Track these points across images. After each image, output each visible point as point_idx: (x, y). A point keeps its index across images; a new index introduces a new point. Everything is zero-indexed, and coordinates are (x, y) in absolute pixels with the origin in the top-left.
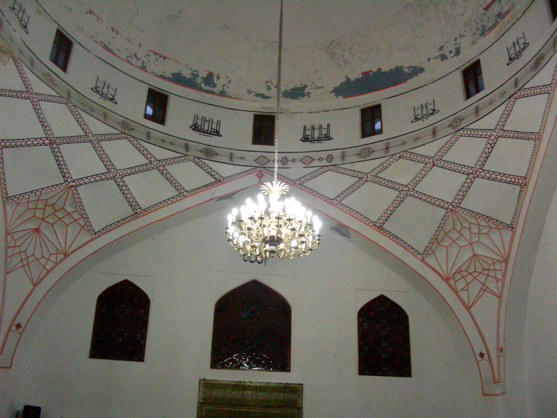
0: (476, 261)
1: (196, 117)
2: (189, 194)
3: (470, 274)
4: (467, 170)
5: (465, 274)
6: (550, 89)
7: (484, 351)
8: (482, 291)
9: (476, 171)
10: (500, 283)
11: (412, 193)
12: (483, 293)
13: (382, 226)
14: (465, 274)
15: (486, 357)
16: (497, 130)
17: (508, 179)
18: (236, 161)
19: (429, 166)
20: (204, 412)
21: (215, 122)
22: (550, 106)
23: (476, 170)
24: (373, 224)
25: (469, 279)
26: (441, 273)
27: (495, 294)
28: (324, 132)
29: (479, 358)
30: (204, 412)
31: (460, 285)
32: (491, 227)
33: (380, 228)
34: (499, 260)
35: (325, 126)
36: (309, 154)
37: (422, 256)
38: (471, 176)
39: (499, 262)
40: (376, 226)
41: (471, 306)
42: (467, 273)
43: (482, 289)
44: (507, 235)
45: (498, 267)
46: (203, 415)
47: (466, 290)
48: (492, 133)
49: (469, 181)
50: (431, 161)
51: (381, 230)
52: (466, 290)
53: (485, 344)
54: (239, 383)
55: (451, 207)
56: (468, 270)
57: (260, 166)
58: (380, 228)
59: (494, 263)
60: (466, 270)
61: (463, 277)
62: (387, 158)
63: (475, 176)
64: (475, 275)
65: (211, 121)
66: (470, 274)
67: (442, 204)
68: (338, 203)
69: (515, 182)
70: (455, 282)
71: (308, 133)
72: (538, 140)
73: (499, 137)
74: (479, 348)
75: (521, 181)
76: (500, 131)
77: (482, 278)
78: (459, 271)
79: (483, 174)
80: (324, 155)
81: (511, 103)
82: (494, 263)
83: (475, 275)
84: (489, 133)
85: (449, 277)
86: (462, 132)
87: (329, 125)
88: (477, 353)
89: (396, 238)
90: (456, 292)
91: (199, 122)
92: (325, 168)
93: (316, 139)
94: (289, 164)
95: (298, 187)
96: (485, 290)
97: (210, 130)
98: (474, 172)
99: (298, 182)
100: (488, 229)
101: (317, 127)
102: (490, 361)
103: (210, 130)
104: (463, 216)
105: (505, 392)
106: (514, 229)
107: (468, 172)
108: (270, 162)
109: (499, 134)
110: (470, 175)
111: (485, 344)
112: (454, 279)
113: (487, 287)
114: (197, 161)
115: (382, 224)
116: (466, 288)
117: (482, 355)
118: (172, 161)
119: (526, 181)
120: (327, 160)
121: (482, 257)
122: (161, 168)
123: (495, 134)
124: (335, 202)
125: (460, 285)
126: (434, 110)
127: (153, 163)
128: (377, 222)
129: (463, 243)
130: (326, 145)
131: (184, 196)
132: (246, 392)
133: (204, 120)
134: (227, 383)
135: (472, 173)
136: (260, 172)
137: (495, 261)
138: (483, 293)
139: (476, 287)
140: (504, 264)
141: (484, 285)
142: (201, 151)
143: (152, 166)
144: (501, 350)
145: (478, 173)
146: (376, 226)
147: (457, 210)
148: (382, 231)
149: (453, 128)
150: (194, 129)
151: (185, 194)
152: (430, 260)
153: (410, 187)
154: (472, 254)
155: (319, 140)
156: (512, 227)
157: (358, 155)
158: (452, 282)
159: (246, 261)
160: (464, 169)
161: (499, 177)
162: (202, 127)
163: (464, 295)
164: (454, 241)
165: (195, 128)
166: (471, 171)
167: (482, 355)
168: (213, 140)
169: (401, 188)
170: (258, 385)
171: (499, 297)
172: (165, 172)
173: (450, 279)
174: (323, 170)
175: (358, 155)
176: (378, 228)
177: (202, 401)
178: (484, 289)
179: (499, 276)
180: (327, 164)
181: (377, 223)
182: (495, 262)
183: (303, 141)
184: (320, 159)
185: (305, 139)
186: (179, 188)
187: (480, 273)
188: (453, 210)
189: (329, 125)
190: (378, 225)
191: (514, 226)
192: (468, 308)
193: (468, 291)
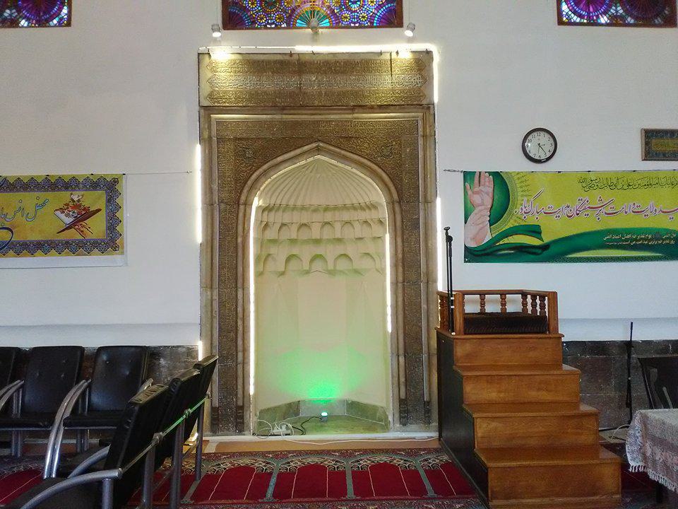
20: (214, 128)
30: (214, 128)
46: (214, 132)
54: (287, 58)
132: (304, 77)
134: (262, 57)
170: (330, 58)
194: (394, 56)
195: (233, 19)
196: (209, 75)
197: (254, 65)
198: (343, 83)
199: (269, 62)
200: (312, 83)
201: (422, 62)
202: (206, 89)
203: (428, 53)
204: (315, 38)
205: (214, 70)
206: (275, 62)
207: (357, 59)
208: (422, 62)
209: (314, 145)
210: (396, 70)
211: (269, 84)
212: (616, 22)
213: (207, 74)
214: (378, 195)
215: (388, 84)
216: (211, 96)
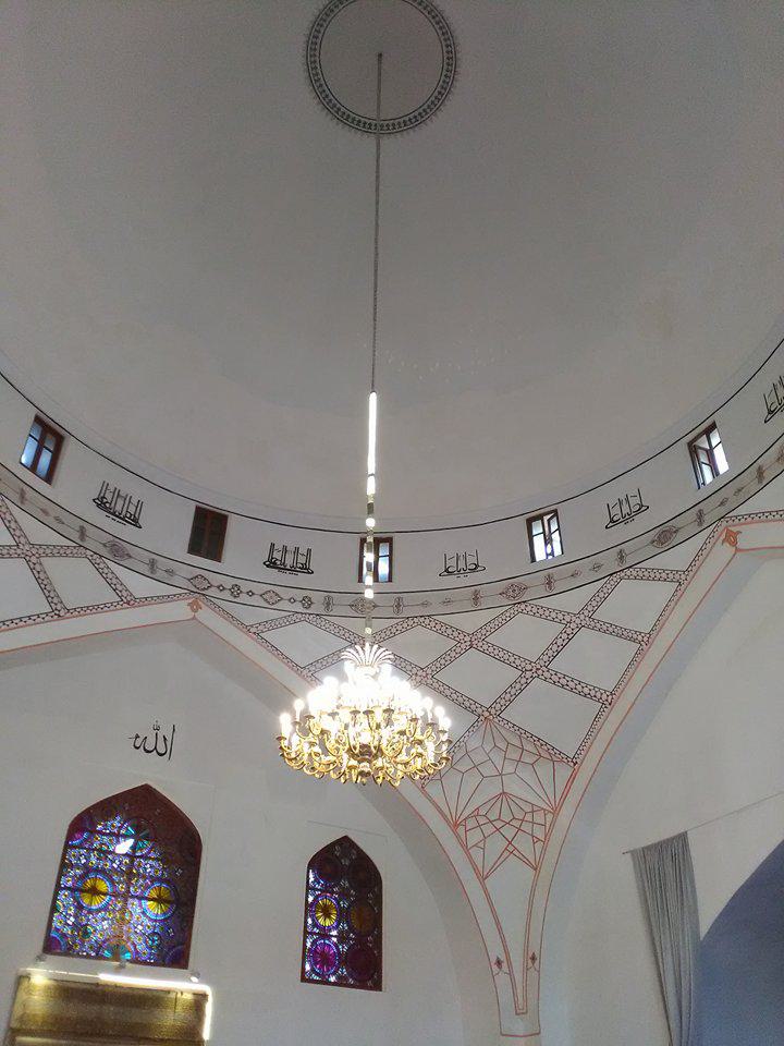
1: (105, 486)
2: (68, 615)
5: (482, 820)
6: (683, 577)
7: (503, 958)
8: (506, 854)
10: (539, 845)
11: (429, 681)
14: (482, 820)
15: (505, 965)
16: (582, 617)
17: (586, 690)
18: (160, 574)
19: (463, 646)
21: (134, 501)
25: (488, 829)
26: (447, 812)
27: (528, 863)
28: (302, 560)
29: (495, 968)
31: (474, 837)
35: (303, 550)
36: (276, 589)
38: (528, 674)
44: (564, 772)
45: (539, 818)
49: (523, 681)
50: (467, 639)
53: (505, 947)
54: (94, 987)
55: (486, 714)
57: (195, 590)
59: (533, 812)
62: (396, 621)
65: (127, 499)
67: (473, 707)
68: (310, 674)
71: (277, 555)
74: (496, 951)
77: (509, 832)
78: (476, 814)
79: (547, 675)
80: (299, 595)
81: (612, 583)
82: (533, 812)
83: (498, 824)
84: (568, 618)
86: (523, 606)
87: (309, 551)
88: (494, 960)
90: (465, 846)
91: (109, 496)
92: (300, 616)
93: (288, 567)
94: (244, 598)
95: (252, 638)
97: (124, 513)
98: (534, 670)
99: (253, 630)
101: (291, 548)
102: (511, 974)
103: (124, 513)
104: (503, 732)
105: (538, 1034)
108: (213, 589)
111: (505, 947)
114: (96, 559)
117: (499, 963)
118: (55, 551)
120: (304, 605)
122: (34, 559)
123: (578, 621)
124: (305, 672)
126: (477, 566)
127: (21, 547)
129: (487, 770)
130: (301, 579)
131: (59, 616)
133: (117, 494)
136: (195, 602)
139: (497, 845)
140: (549, 817)
141: (510, 843)
142: (105, 545)
143: (19, 551)
145: (540, 672)
147: (496, 720)
149: (508, 597)
150: (98, 505)
151: (62, 613)
152: (434, 790)
153: (429, 671)
155: (293, 570)
157: (351, 606)
158: (461, 830)
159: (138, 748)
161: (572, 684)
162: (113, 505)
163: (477, 854)
165: (101, 503)
166: (529, 667)
167: (499, 963)
168: (126, 532)
169: (414, 671)
171: (535, 869)
172: (38, 567)
174: (291, 619)
175: (351, 606)
177: (15, 1025)
178: (510, 848)
180: (301, 610)
183: (268, 566)
184: (292, 600)
185: (271, 564)
186: (55, 600)
189: (309, 551)
191: (578, 761)
192: (482, 878)
194: (179, 995)
195: (53, 945)
196: (25, 997)
197: (66, 992)
198: (136, 1016)
199: (77, 990)
200: (110, 1011)
201: (200, 999)
202: (18, 1011)
203: (204, 996)
204: (119, 970)
205: (29, 992)
206: (83, 990)
207: (149, 994)
208: (200, 999)
210: (179, 1009)
211: (74, 1011)
212: (341, 982)
213: (22, 995)
215: (170, 1019)
216: (21, 1019)
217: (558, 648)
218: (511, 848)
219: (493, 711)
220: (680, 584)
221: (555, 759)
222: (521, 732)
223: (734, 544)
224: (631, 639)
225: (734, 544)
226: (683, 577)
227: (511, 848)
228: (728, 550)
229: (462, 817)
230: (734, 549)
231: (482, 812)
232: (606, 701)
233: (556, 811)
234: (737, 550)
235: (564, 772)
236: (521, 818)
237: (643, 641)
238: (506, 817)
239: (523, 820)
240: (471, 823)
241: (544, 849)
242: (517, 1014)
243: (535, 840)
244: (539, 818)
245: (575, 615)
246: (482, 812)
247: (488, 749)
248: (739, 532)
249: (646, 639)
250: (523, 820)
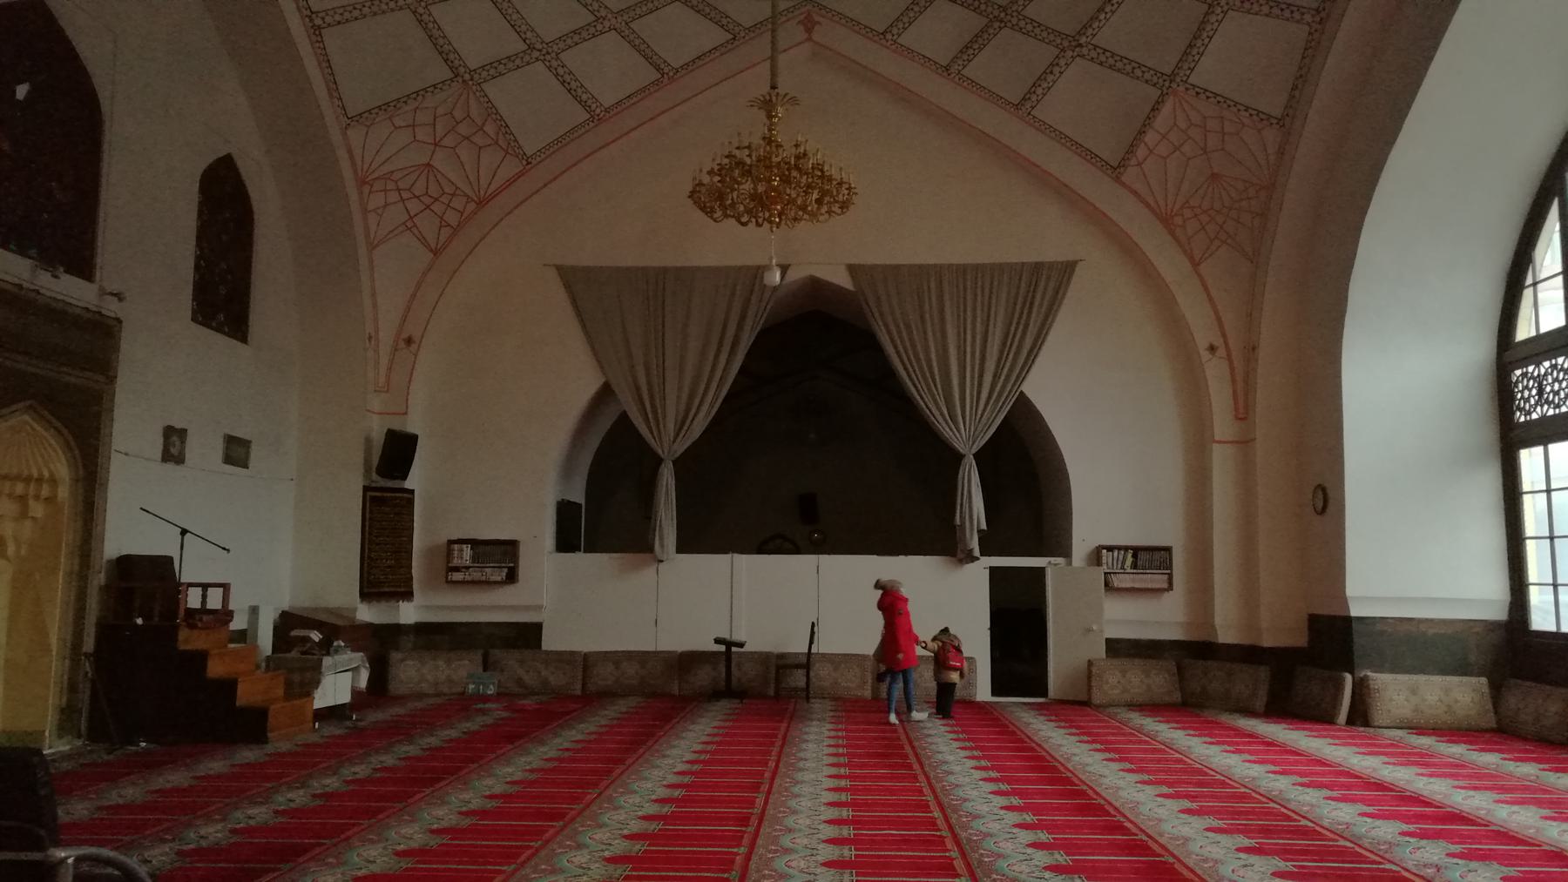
0: (423, 177)
3: (399, 190)
4: (534, 40)
7: (373, 334)
9: (548, 53)
10: (445, 232)
12: (402, 232)
13: (324, 28)
16: (619, 20)
22: (725, 53)
23: (550, 50)
24: (308, 13)
25: (394, 196)
27: (427, 246)
32: (497, 143)
33: (315, 30)
34: (466, 195)
37: (349, 121)
38: (535, 54)
39: (465, 199)
40: (311, 20)
41: (377, 245)
42: (410, 195)
43: (404, 223)
47: (378, 214)
48: (610, 16)
51: (314, 33)
52: (378, 214)
55: (467, 77)
56: (399, 183)
58: (316, 32)
59: (453, 195)
60: (396, 182)
61: (385, 191)
63: (542, 58)
64: (405, 195)
66: (399, 190)
69: (590, 107)
70: (370, 192)
72: (669, 79)
73: (615, 29)
75: (598, 111)
76: (623, 23)
77: (414, 206)
82: (453, 195)
83: (405, 195)
85: (367, 180)
89: (325, 62)
90: (365, 211)
96: (409, 229)
98: (544, 51)
100: (489, 142)
106: (530, 166)
107: (534, 44)
109: (618, 26)
110: (534, 51)
112: (372, 186)
113: (415, 226)
115: (325, 25)
116: (380, 211)
117: (370, 338)
119: (604, 116)
121: (439, 176)
125: (376, 201)
128: (320, 15)
135: (540, 50)
137: (458, 192)
138: (402, 232)
144: (409, 341)
145: (548, 57)
146: (311, 20)
147: (474, 87)
148: (314, 38)
152: (355, 135)
154: (425, 160)
156: (528, 162)
158: (366, 189)
160: (529, 35)
163: (372, 219)
164: (414, 126)
166: (539, 46)
173: (367, 183)
176: (312, 27)
179: (452, 218)
181: (317, 16)
182: (458, 195)
187: (415, 197)
188: (468, 84)
190: (318, 22)
191: (534, 162)
193: (381, 216)
209: (28, 403)
214: (63, 470)
217: (576, 37)
218: (409, 224)
219: (476, 76)
220: (734, 39)
221: (510, 151)
222: (492, 111)
223: (809, 30)
224: (658, 69)
225: (809, 30)
226: (742, 34)
227: (409, 224)
228: (800, 34)
229: (376, 175)
230: (806, 36)
231: (396, 176)
232: (596, 116)
233: (482, 203)
234: (809, 39)
235: (510, 168)
236: (435, 196)
237: (665, 74)
238: (419, 189)
239: (436, 200)
240: (378, 185)
241: (450, 240)
242: (387, 391)
243: (443, 224)
244: (458, 203)
245: (612, 12)
246: (396, 176)
247: (440, 111)
248: (819, 23)
249: (671, 74)
250: (436, 200)
